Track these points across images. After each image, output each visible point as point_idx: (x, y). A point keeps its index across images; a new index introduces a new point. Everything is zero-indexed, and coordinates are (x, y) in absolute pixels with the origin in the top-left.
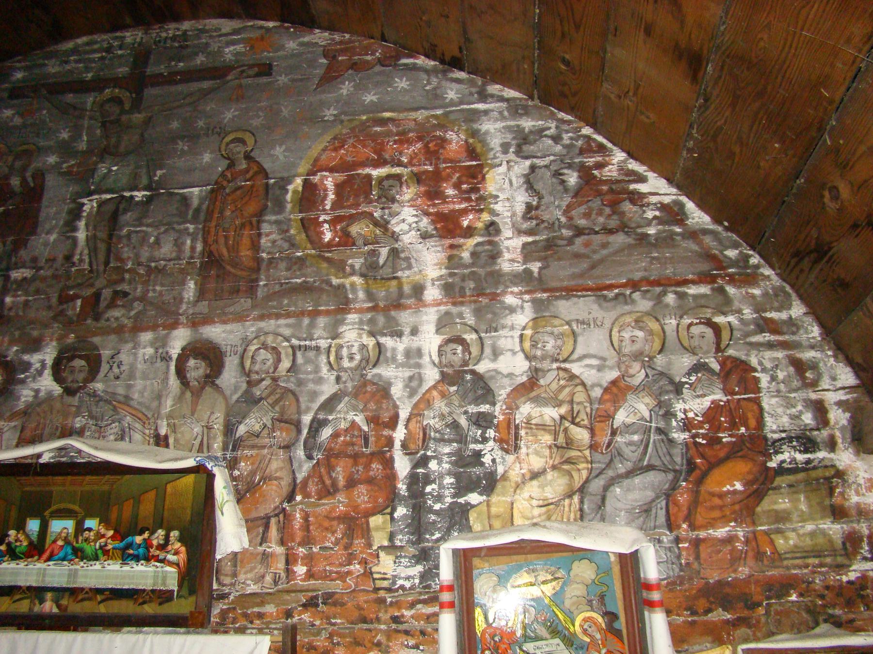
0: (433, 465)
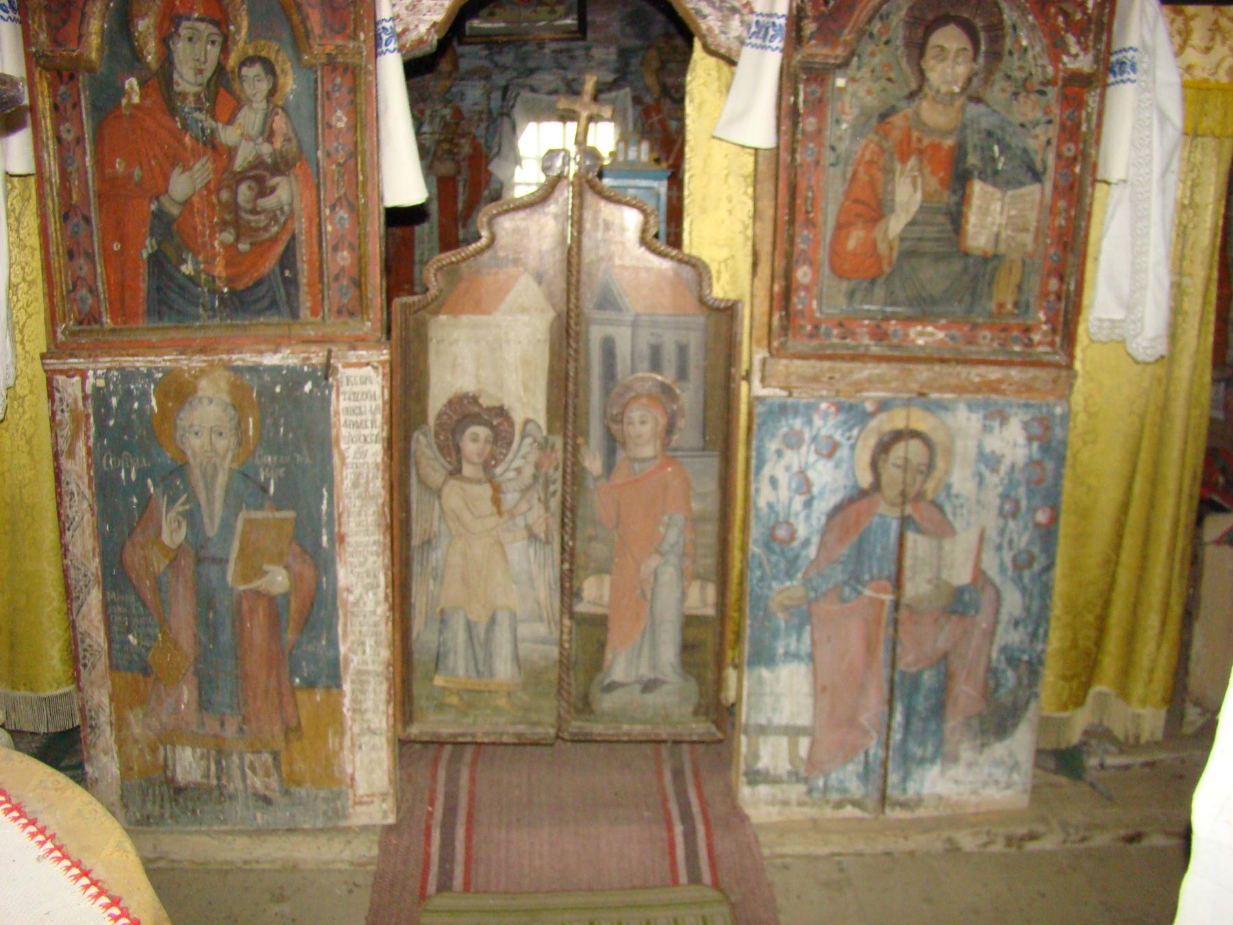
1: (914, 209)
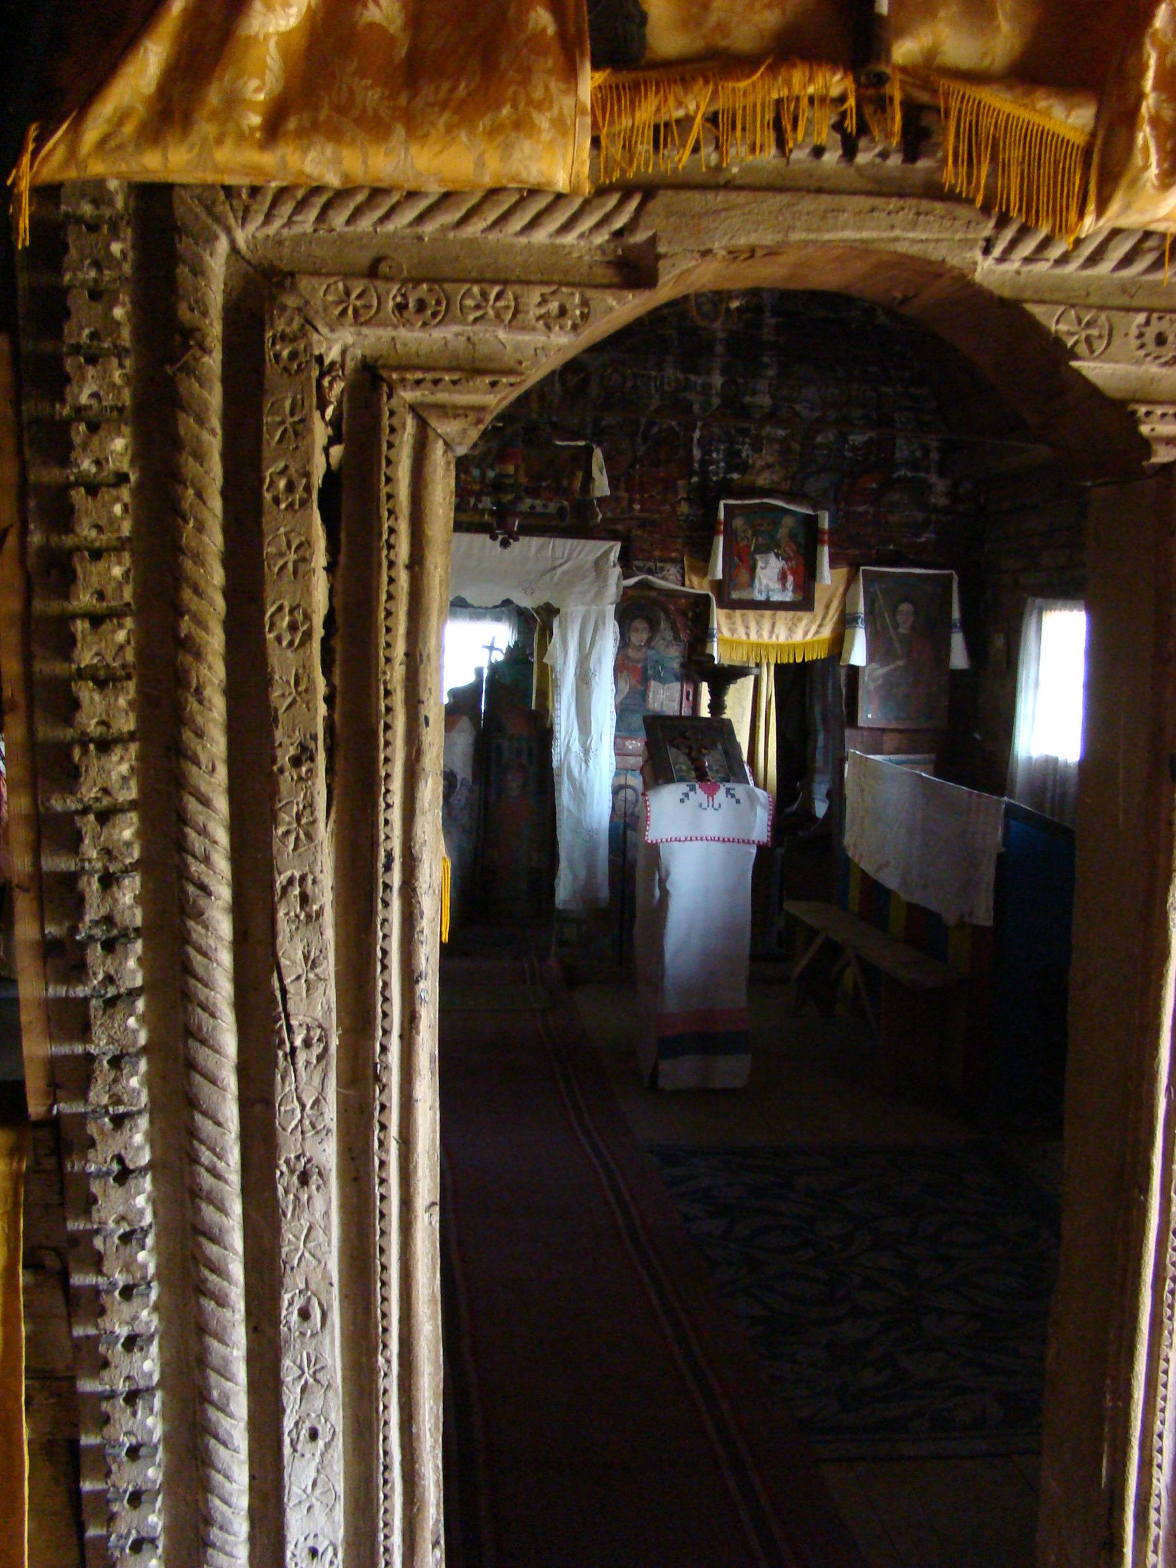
0: (714, 455)
1: (626, 692)
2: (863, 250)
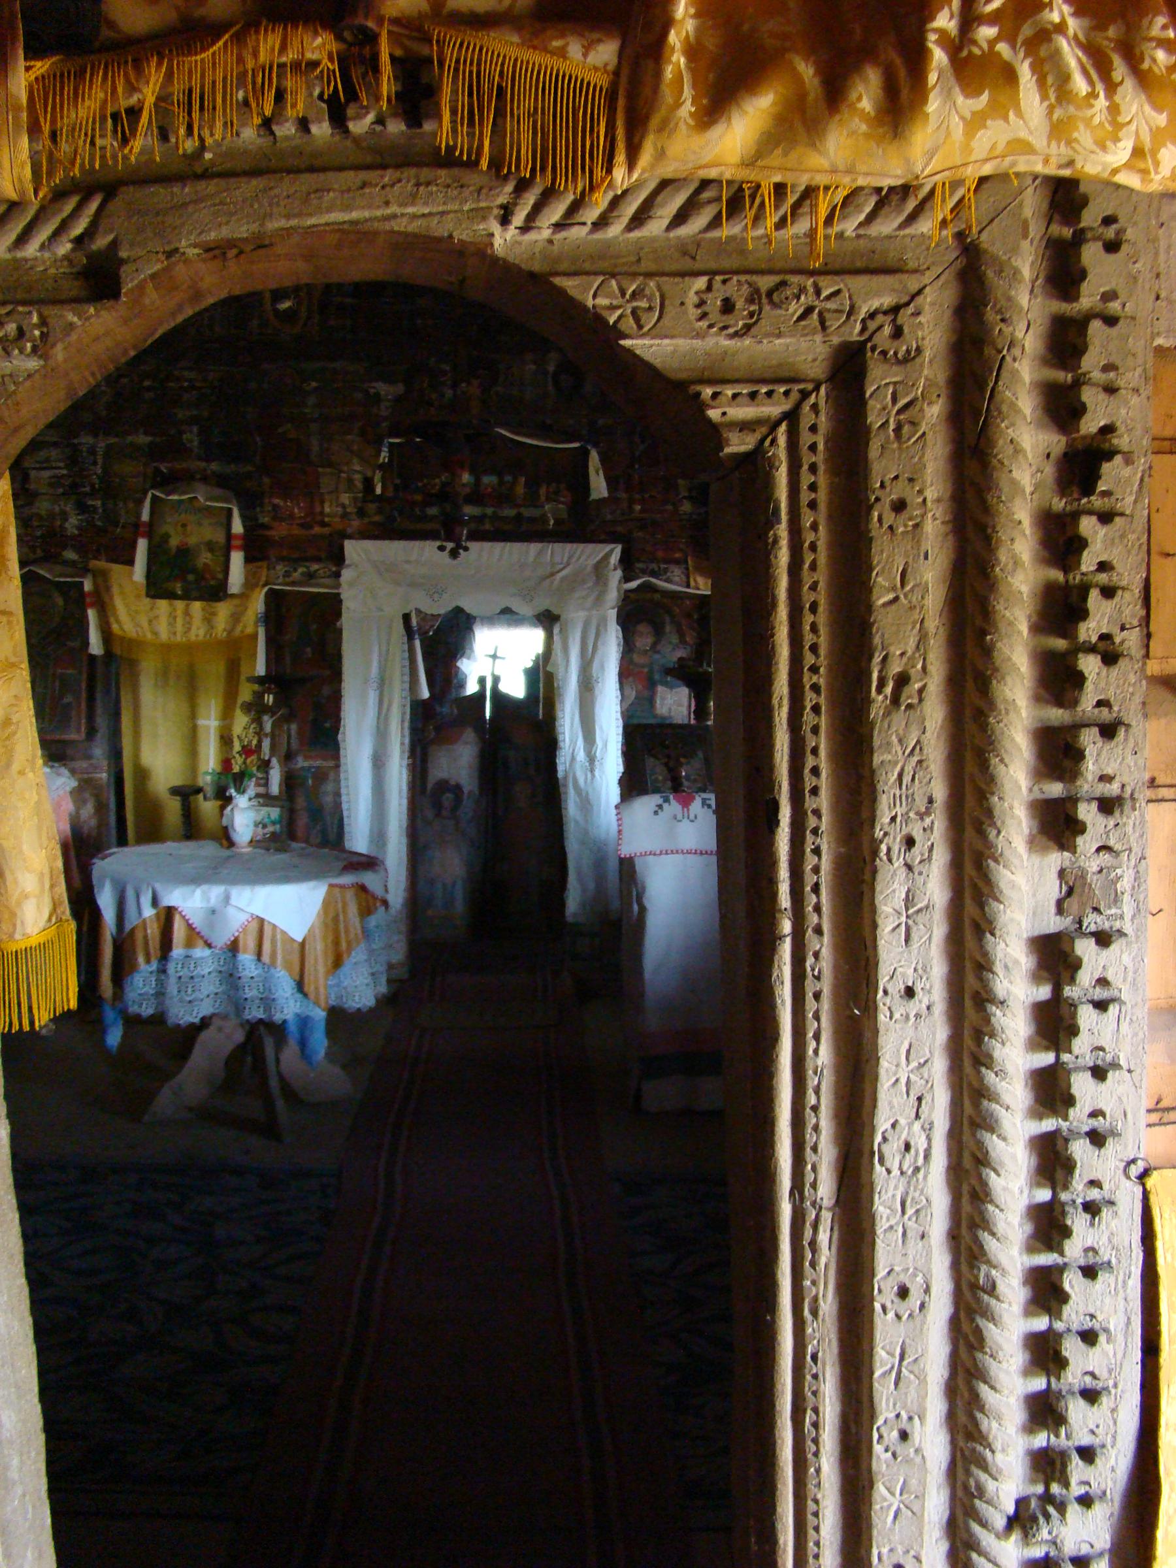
2: (356, 234)
